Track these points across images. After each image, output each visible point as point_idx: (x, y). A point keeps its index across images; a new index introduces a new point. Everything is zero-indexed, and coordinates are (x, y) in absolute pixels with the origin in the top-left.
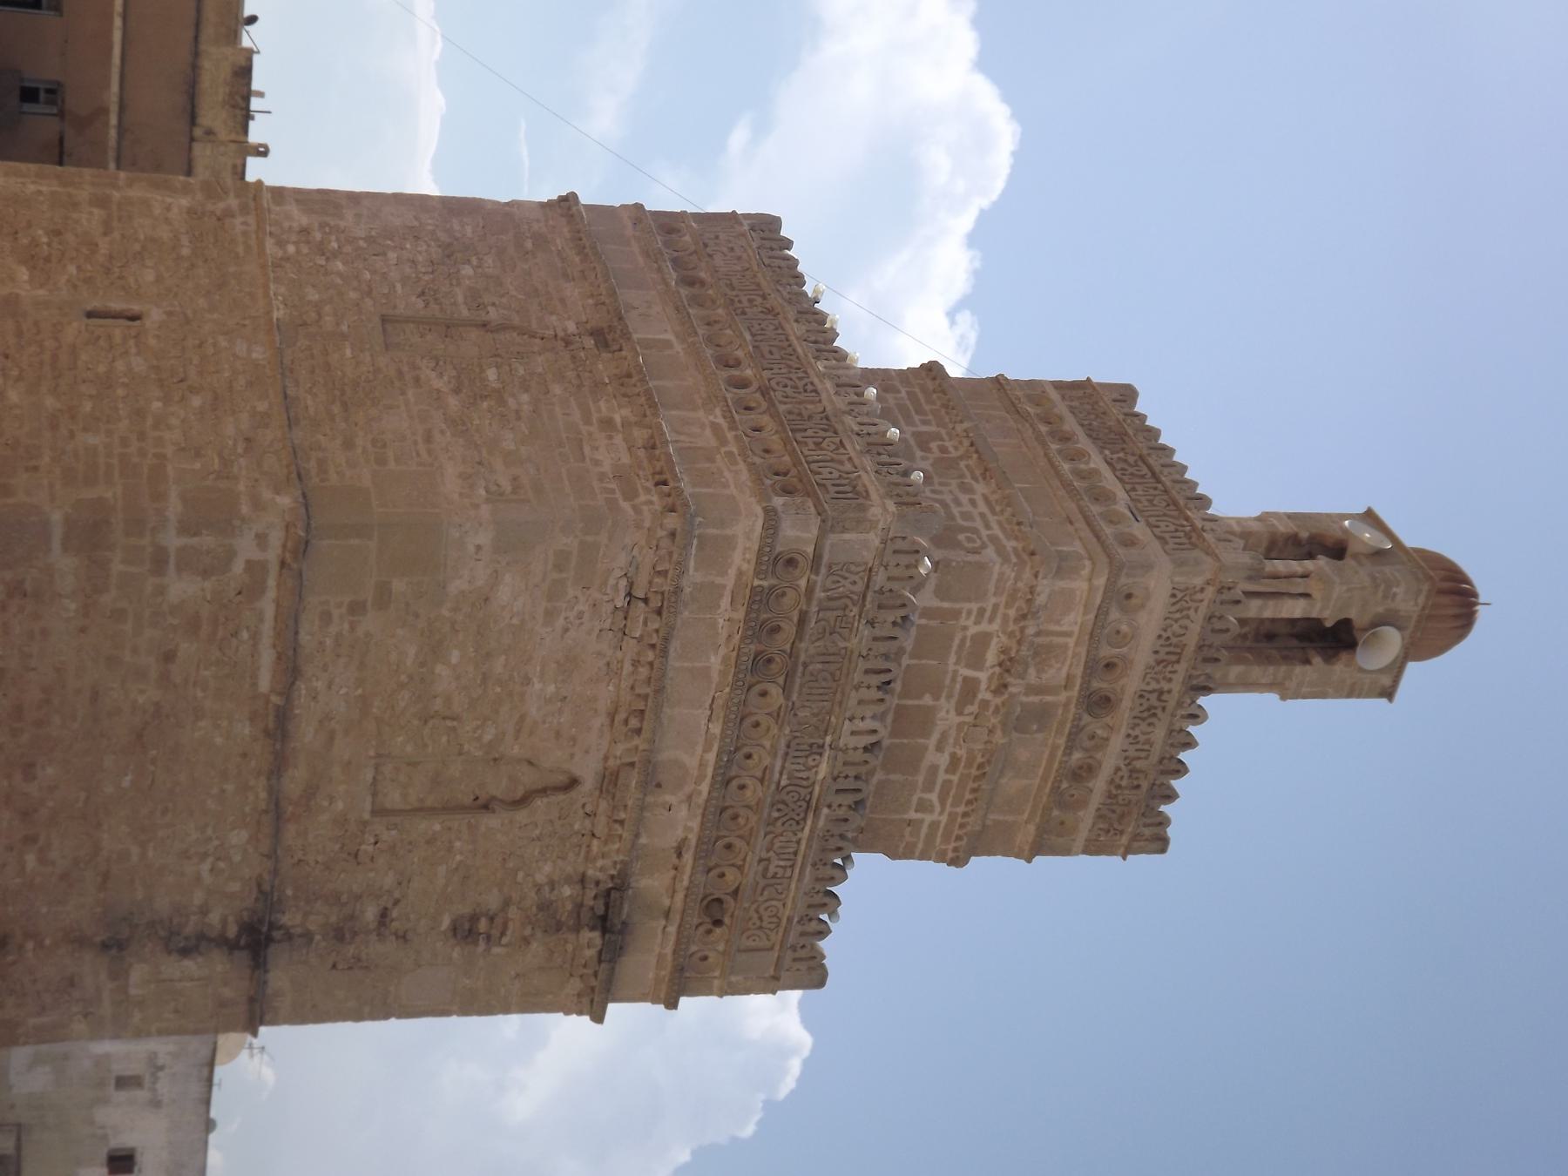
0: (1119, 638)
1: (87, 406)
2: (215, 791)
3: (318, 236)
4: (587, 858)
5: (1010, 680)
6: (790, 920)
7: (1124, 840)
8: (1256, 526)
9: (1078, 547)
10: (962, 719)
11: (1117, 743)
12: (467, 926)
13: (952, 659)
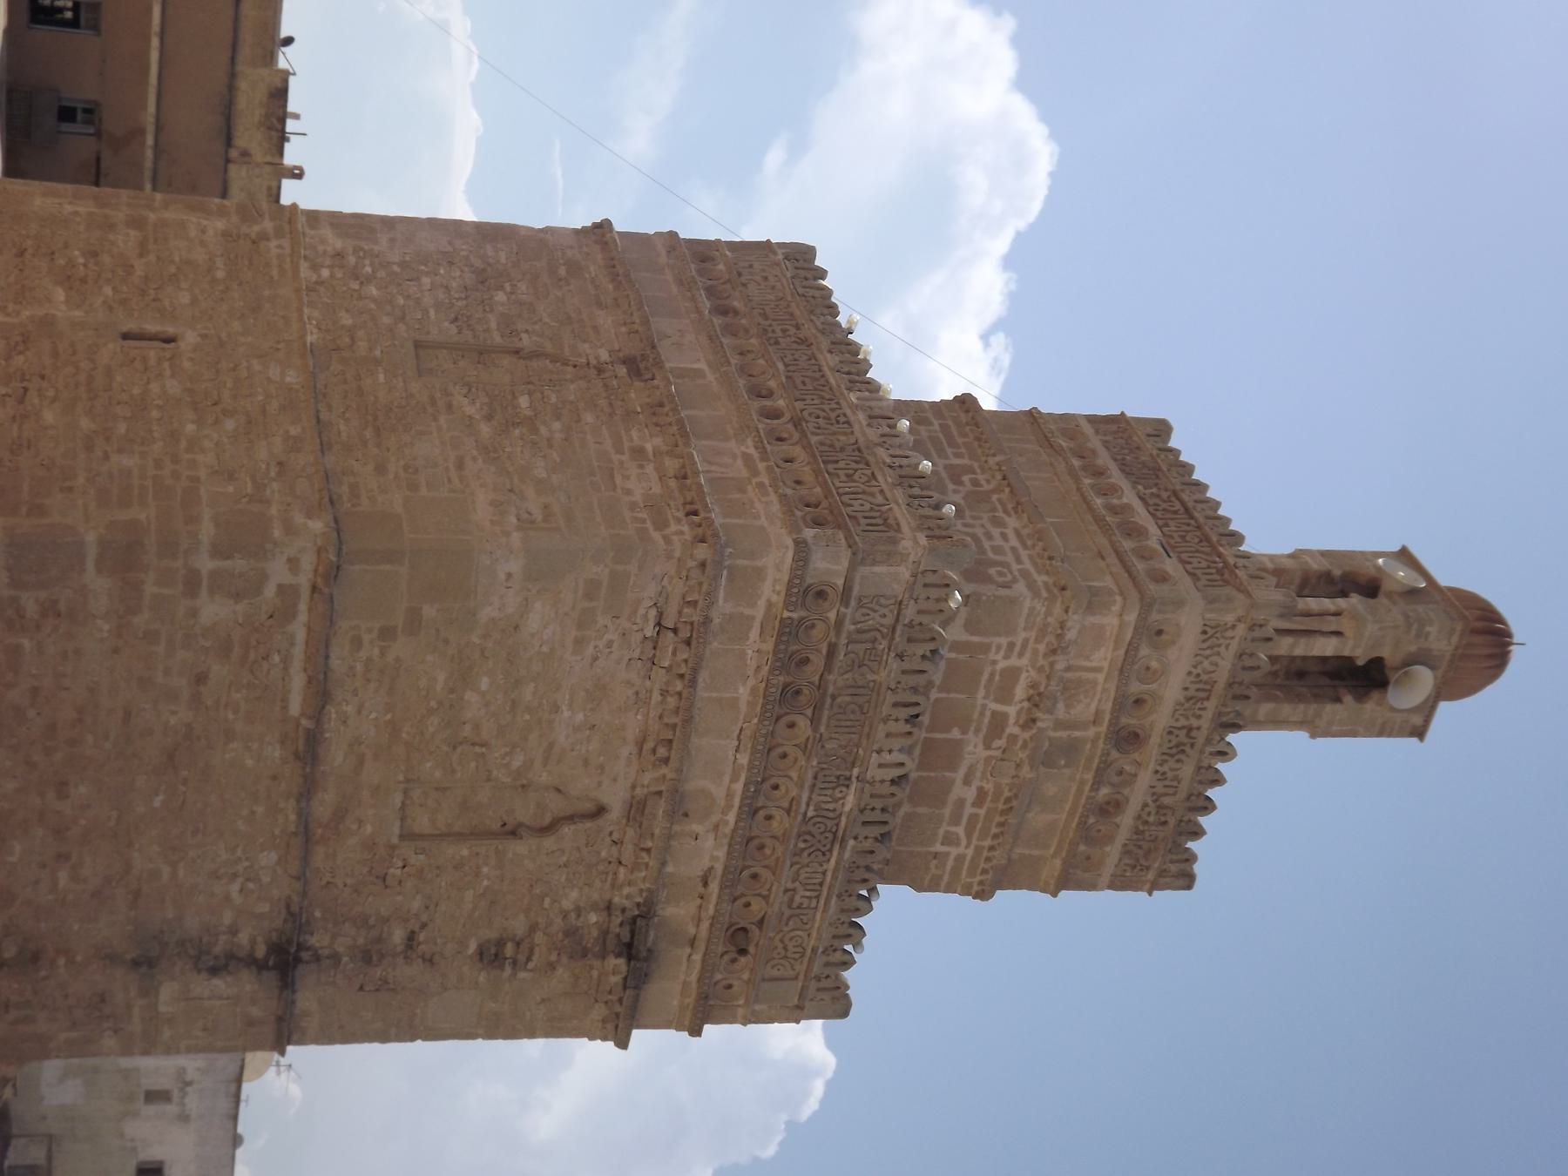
0: (1149, 674)
1: (122, 428)
2: (245, 812)
3: (352, 260)
4: (613, 886)
5: (1039, 715)
6: (814, 950)
7: (1151, 876)
8: (1289, 564)
9: (1108, 582)
10: (989, 753)
11: (1145, 779)
12: (493, 951)
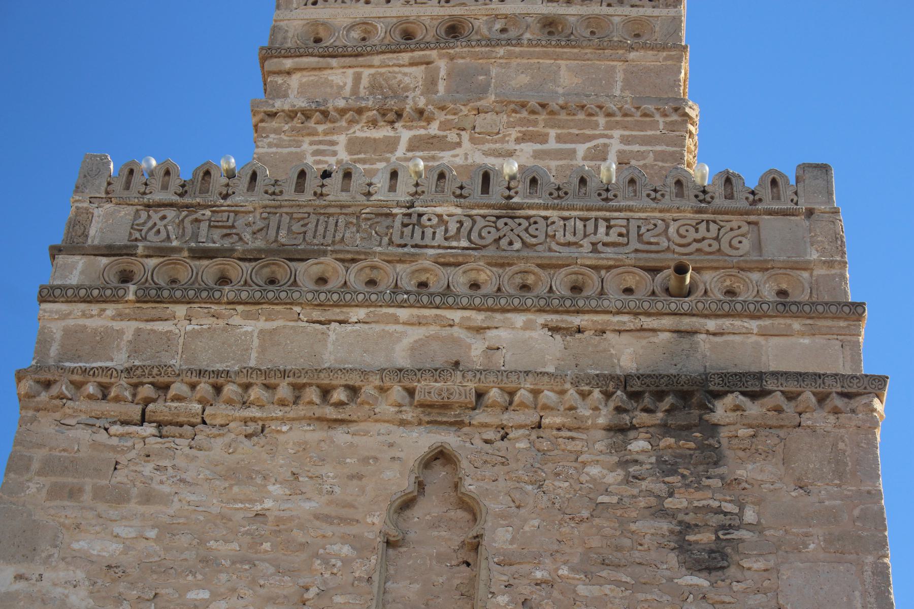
4: (578, 429)
5: (408, 108)
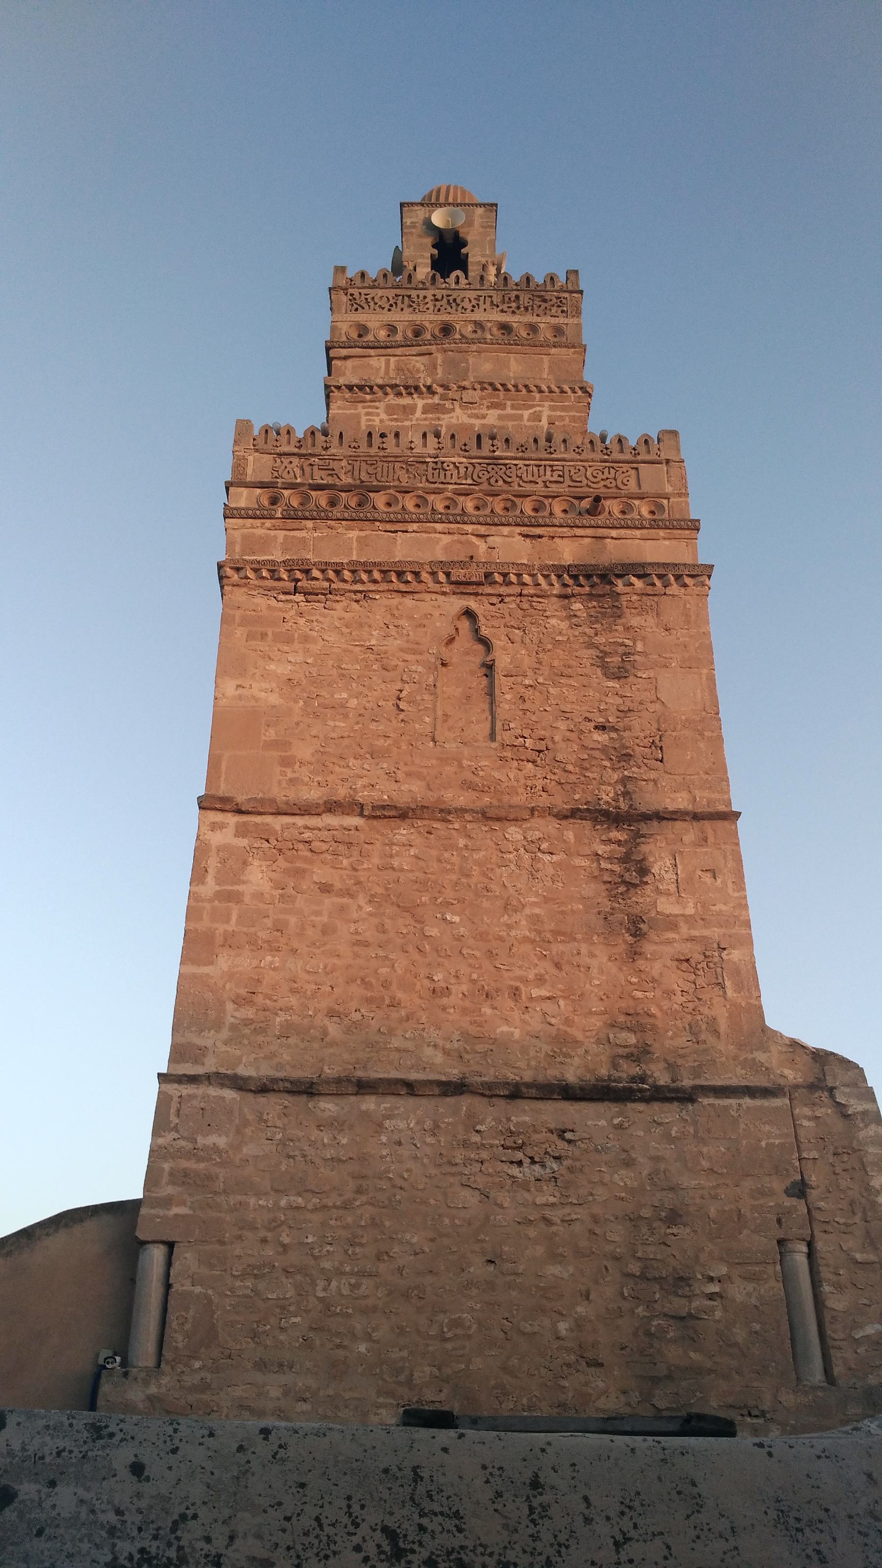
13: (407, 423)
